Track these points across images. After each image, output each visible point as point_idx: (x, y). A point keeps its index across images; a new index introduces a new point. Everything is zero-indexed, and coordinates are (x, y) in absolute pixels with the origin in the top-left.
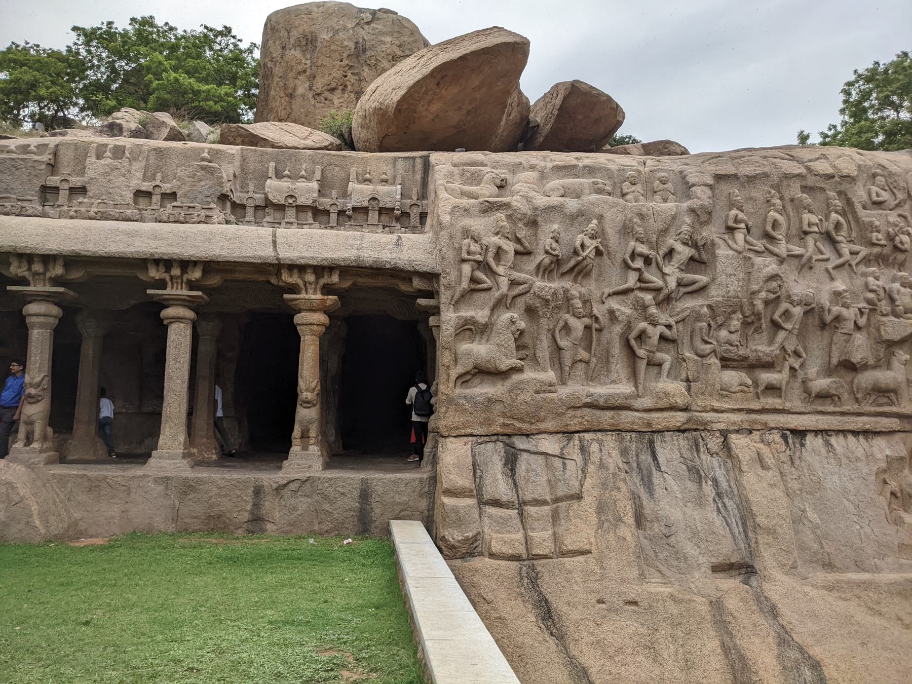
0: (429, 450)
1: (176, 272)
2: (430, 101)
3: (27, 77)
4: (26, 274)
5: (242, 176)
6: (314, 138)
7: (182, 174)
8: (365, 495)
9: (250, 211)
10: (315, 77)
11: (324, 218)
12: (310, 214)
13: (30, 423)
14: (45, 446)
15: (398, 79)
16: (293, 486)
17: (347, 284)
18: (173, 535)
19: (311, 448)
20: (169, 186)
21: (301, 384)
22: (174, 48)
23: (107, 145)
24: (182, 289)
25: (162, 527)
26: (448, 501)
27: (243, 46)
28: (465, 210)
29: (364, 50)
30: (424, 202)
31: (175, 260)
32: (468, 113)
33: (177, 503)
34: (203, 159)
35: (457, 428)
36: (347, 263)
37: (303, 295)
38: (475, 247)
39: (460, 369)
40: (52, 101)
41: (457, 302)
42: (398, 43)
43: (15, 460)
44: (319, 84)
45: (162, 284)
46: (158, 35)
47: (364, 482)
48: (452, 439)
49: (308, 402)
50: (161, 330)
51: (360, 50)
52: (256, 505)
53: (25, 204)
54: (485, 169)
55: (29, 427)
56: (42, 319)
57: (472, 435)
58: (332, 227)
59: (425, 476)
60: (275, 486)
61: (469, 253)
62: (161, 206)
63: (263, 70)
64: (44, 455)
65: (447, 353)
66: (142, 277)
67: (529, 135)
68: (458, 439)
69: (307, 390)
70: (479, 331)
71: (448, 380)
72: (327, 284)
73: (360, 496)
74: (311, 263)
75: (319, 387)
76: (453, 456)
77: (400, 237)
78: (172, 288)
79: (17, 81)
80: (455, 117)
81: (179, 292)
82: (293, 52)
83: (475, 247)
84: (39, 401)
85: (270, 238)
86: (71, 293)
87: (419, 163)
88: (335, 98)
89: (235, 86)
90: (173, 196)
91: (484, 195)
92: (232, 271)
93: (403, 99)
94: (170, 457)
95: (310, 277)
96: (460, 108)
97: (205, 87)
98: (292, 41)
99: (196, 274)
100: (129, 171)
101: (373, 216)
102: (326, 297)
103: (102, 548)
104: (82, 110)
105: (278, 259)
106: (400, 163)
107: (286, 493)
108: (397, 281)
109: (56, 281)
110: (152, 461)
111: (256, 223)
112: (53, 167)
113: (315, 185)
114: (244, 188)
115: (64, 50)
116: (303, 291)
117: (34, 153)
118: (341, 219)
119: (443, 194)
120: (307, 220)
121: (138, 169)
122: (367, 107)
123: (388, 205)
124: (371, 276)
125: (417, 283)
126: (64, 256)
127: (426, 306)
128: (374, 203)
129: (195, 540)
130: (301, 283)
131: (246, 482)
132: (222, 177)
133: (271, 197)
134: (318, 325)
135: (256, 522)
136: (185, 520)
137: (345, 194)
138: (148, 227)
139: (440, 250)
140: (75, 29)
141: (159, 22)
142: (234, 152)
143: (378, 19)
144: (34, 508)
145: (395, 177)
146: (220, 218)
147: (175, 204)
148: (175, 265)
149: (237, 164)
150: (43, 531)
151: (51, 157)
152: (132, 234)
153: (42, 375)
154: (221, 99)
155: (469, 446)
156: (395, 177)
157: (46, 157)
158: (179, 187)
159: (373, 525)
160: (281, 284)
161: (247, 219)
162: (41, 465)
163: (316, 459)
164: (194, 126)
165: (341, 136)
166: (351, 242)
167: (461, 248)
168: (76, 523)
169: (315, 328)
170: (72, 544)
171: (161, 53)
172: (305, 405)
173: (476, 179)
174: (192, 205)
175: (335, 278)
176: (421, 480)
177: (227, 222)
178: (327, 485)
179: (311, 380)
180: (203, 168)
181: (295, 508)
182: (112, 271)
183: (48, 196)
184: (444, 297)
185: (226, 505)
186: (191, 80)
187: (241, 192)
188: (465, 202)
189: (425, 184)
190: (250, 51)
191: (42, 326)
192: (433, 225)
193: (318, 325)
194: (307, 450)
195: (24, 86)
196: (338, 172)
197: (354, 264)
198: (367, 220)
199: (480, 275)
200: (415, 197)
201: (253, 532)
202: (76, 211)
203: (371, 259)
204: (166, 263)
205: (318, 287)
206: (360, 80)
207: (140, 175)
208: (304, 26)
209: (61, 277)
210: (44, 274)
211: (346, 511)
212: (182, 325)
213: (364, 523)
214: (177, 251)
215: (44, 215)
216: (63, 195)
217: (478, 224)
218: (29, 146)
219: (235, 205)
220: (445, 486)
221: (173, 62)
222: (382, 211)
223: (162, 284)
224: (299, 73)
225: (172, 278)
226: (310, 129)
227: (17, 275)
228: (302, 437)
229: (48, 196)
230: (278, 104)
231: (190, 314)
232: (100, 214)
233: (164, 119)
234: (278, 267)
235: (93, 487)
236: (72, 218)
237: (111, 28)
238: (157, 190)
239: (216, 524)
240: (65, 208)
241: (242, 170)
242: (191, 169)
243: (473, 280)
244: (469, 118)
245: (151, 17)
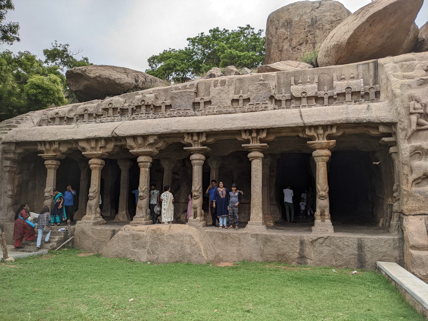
0: (396, 223)
1: (254, 135)
2: (366, 35)
3: (172, 62)
4: (191, 142)
5: (278, 86)
6: (301, 66)
7: (252, 89)
8: (360, 247)
9: (283, 103)
11: (321, 101)
12: (314, 100)
13: (195, 208)
14: (202, 219)
15: (347, 27)
16: (320, 241)
17: (340, 134)
18: (261, 263)
19: (326, 221)
20: (246, 95)
21: (319, 187)
22: (228, 39)
23: (218, 81)
24: (257, 143)
25: (256, 259)
26: (414, 252)
27: (256, 32)
28: (409, 85)
30: (378, 86)
31: (254, 129)
32: (388, 38)
33: (262, 247)
34: (261, 80)
35: (415, 210)
36: (341, 122)
37: (317, 141)
38: (418, 105)
39: (415, 176)
40: (182, 71)
41: (409, 138)
43: (190, 225)
45: (248, 141)
46: (221, 35)
47: (359, 240)
48: (412, 217)
49: (323, 197)
50: (249, 163)
52: (302, 250)
53: (187, 111)
54: (416, 62)
55: (195, 210)
56: (198, 161)
57: (424, 214)
58: (326, 105)
59: (396, 237)
60: (310, 240)
61: (414, 109)
62: (243, 105)
63: (268, 41)
64: (202, 223)
65: (406, 167)
66: (239, 139)
67: (418, 46)
68: (415, 217)
69: (322, 190)
70: (424, 153)
71: (407, 183)
72: (330, 134)
73: (358, 248)
74: (321, 124)
75: (328, 189)
76: (414, 226)
77: (369, 105)
78: (253, 143)
79: (169, 64)
80: (379, 42)
81: (256, 144)
82: (281, 30)
83: (418, 105)
84: (198, 198)
85: (299, 114)
86: (209, 149)
87: (372, 66)
88: (302, 48)
89: (255, 51)
90: (248, 100)
91: (418, 76)
92: (280, 132)
93: (352, 36)
94: (257, 224)
95: (321, 131)
96: (383, 36)
97: (243, 54)
99: (264, 135)
100: (228, 91)
101: (348, 97)
102: (330, 141)
103: (233, 268)
104: (192, 73)
105: (304, 124)
106: (361, 67)
107: (317, 244)
108: (369, 129)
109: (203, 144)
110: (248, 226)
111: (287, 108)
112: (196, 93)
113: (315, 85)
114: (280, 92)
115: (184, 49)
116: (317, 139)
117: (189, 88)
118: (330, 101)
119: (393, 79)
120: (312, 103)
121: (232, 88)
122: (329, 45)
123: (357, 90)
124: (353, 128)
125: (382, 129)
126: (206, 132)
127: (388, 142)
128: (348, 90)
129: (273, 266)
130: (315, 135)
131: (296, 238)
132: (270, 88)
133: (294, 94)
134: (326, 156)
135: (302, 258)
136: (267, 256)
137: (332, 87)
138: (240, 115)
139: (397, 109)
140: (188, 39)
141: (221, 29)
142: (274, 75)
143: (323, 5)
144: (202, 247)
145: (358, 75)
146: (271, 107)
147: (250, 103)
148: (254, 131)
149: (276, 80)
150: (206, 258)
151: (196, 89)
152: (234, 119)
153: (199, 187)
154: (250, 58)
155: (423, 221)
156: (358, 75)
157: (194, 90)
158: (251, 95)
159: (367, 264)
160: (305, 136)
161: (282, 107)
162: (201, 227)
163: (330, 227)
164: (244, 70)
165: (312, 64)
166: (341, 111)
167: (409, 107)
168: (217, 256)
169: (324, 158)
170: (218, 265)
171: (223, 42)
172: (322, 198)
173: (411, 68)
174: (258, 103)
175: (334, 131)
176: (394, 240)
177: (274, 109)
178: (338, 240)
179: (324, 185)
180: (261, 84)
181: (322, 252)
182: (225, 137)
183: (196, 107)
184: (401, 135)
185: (286, 249)
186: (237, 51)
187: (279, 94)
188: (407, 81)
189: (376, 76)
190: (259, 34)
191: (198, 164)
192: (387, 97)
193: (326, 156)
194: (324, 221)
195: (171, 67)
196: (327, 77)
197: (345, 122)
198: (345, 99)
199: (422, 121)
200: (371, 84)
201: (301, 264)
202: (208, 112)
203: (355, 119)
204: (249, 131)
205: (325, 136)
207: (233, 92)
209: (205, 141)
210: (198, 141)
211: (350, 255)
212: (258, 160)
213: (361, 262)
214: (255, 125)
215: (195, 115)
216: (202, 105)
217: (418, 92)
218: (187, 85)
219: (276, 101)
220: (411, 243)
221: (228, 45)
222: (353, 94)
223: (248, 141)
225: (252, 138)
226: (298, 62)
227: (187, 142)
228: (321, 215)
229: (196, 107)
230: (275, 56)
231: (261, 155)
232: (218, 112)
233: (232, 69)
234: (304, 128)
235: (224, 238)
236: (207, 115)
237: (202, 35)
238: (241, 98)
239: (282, 259)
240: (203, 111)
241: (278, 83)
242: (256, 86)
243: (418, 124)
244: (388, 41)
245: (218, 28)
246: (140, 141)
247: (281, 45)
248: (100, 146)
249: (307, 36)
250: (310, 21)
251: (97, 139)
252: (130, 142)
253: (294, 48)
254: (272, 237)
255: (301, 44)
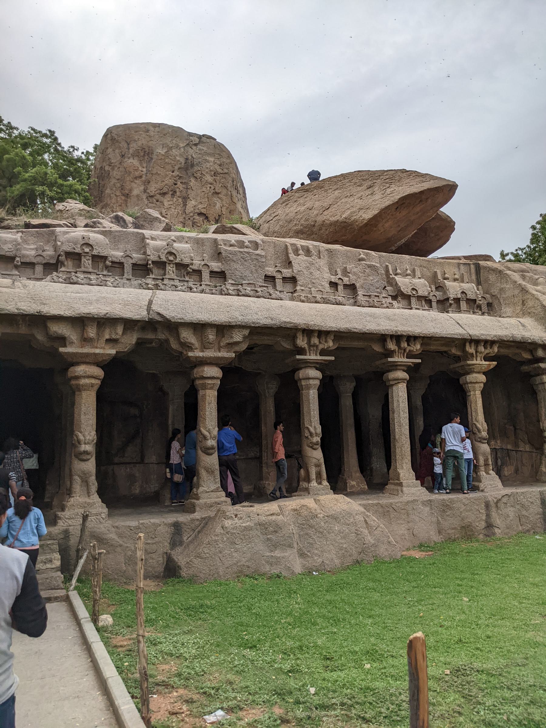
10: (149, 182)
29: (192, 166)
42: (218, 162)
44: (153, 188)
51: (189, 166)
98: (131, 151)
206: (187, 188)
208: (142, 141)
214: (410, 329)
224: (136, 178)
246: (211, 336)
247: (128, 186)
248: (107, 337)
249: (176, 184)
250: (182, 160)
251: (104, 322)
252: (187, 335)
253: (152, 196)
254: (452, 501)
255: (164, 194)
